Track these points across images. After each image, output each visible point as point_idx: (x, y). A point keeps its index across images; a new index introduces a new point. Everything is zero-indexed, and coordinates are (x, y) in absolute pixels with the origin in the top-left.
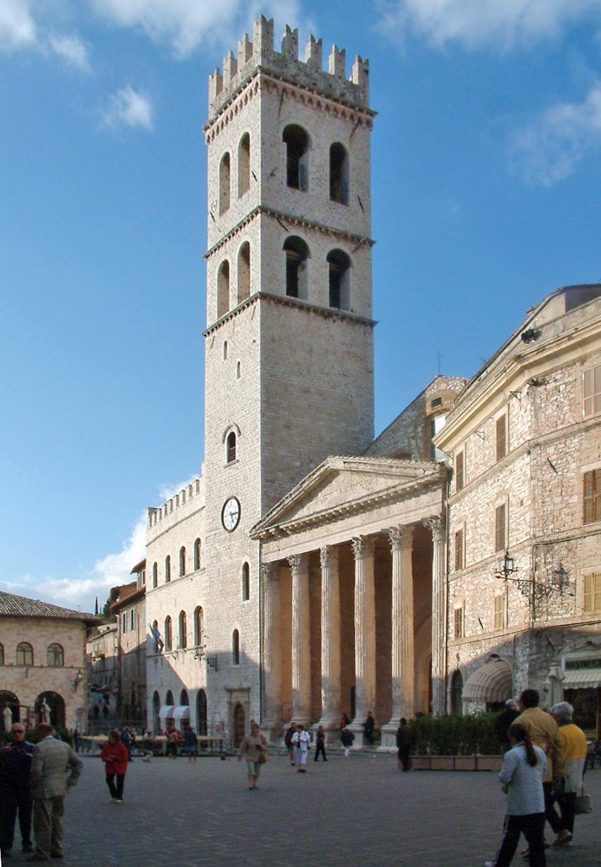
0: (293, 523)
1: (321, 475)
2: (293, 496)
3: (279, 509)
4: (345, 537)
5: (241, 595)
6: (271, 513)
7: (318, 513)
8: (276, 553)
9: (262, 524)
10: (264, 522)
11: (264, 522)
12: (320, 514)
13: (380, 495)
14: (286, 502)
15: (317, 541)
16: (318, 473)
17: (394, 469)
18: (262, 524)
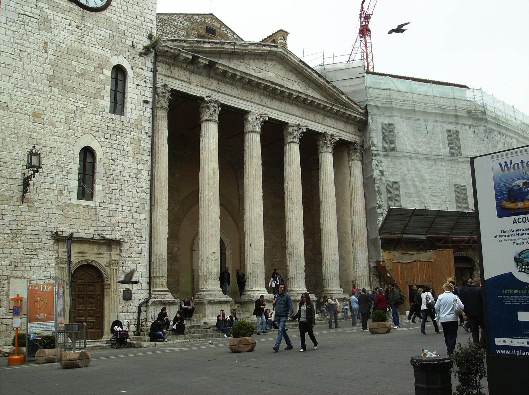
0: (238, 73)
1: (270, 52)
2: (236, 47)
3: (215, 46)
4: (283, 117)
5: (106, 102)
6: (204, 42)
7: (273, 83)
8: (185, 84)
9: (185, 45)
10: (188, 45)
11: (188, 45)
12: (274, 86)
13: (334, 107)
14: (226, 47)
15: (249, 104)
16: (269, 49)
17: (344, 97)
18: (185, 45)
